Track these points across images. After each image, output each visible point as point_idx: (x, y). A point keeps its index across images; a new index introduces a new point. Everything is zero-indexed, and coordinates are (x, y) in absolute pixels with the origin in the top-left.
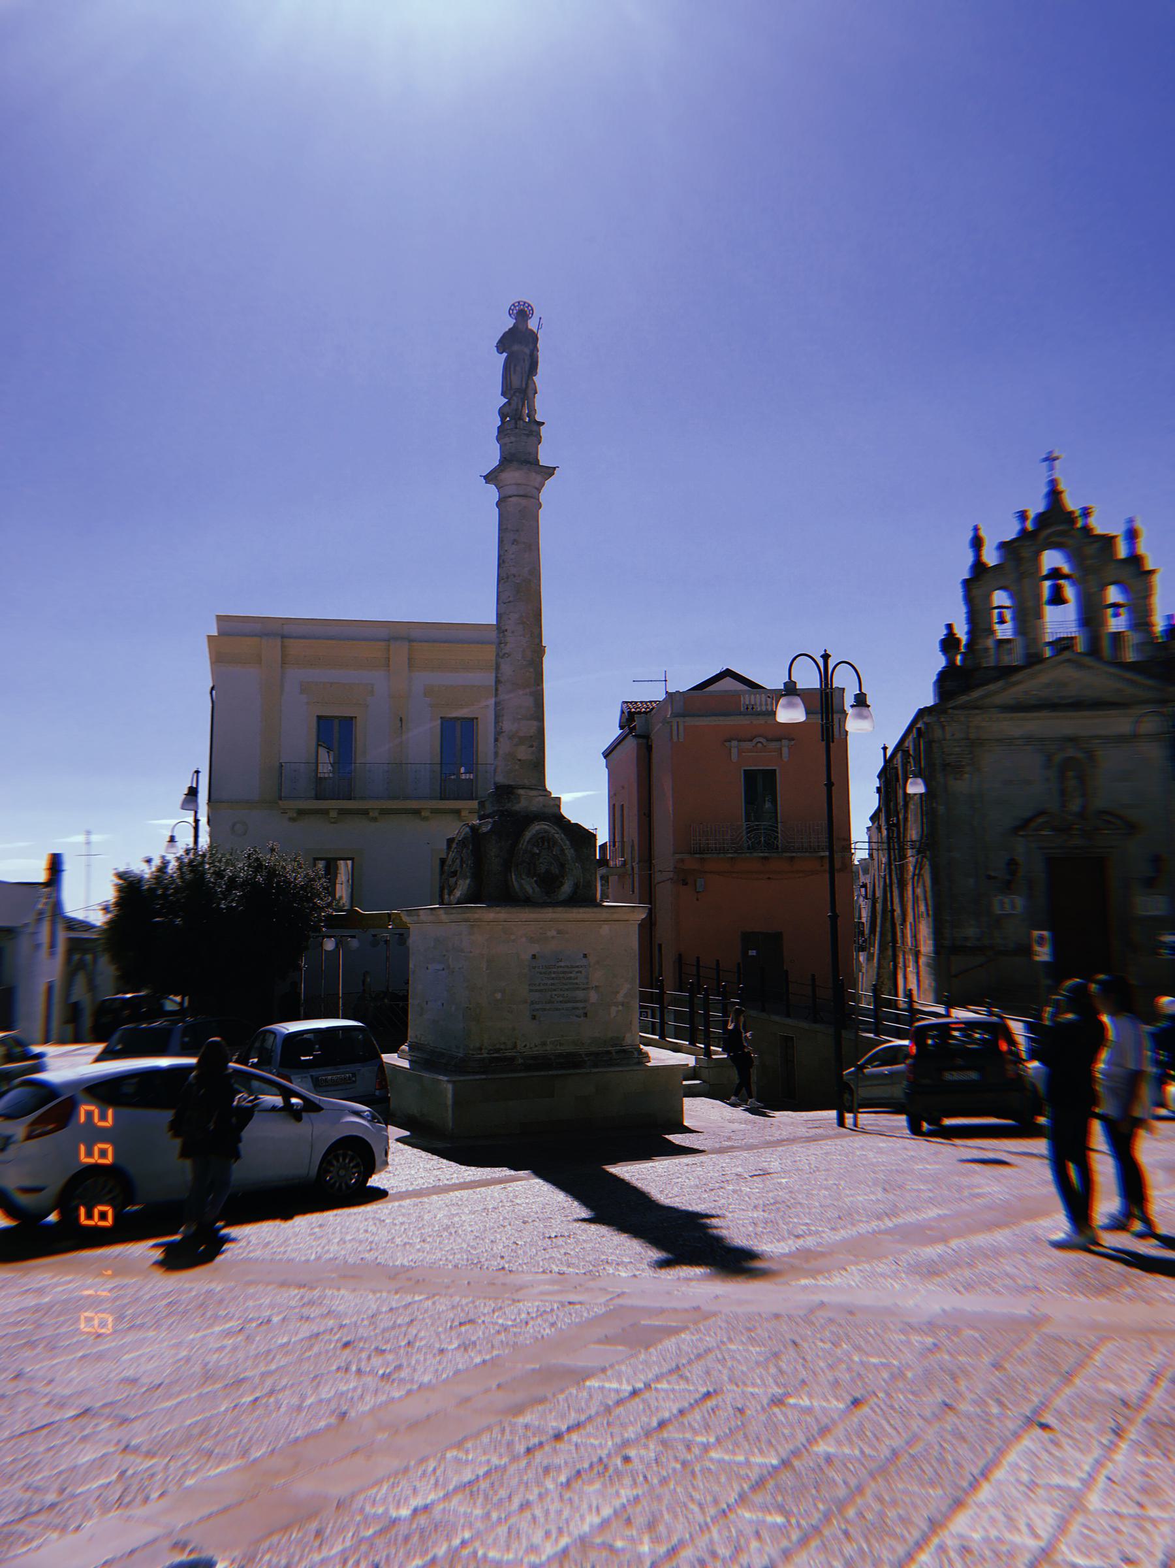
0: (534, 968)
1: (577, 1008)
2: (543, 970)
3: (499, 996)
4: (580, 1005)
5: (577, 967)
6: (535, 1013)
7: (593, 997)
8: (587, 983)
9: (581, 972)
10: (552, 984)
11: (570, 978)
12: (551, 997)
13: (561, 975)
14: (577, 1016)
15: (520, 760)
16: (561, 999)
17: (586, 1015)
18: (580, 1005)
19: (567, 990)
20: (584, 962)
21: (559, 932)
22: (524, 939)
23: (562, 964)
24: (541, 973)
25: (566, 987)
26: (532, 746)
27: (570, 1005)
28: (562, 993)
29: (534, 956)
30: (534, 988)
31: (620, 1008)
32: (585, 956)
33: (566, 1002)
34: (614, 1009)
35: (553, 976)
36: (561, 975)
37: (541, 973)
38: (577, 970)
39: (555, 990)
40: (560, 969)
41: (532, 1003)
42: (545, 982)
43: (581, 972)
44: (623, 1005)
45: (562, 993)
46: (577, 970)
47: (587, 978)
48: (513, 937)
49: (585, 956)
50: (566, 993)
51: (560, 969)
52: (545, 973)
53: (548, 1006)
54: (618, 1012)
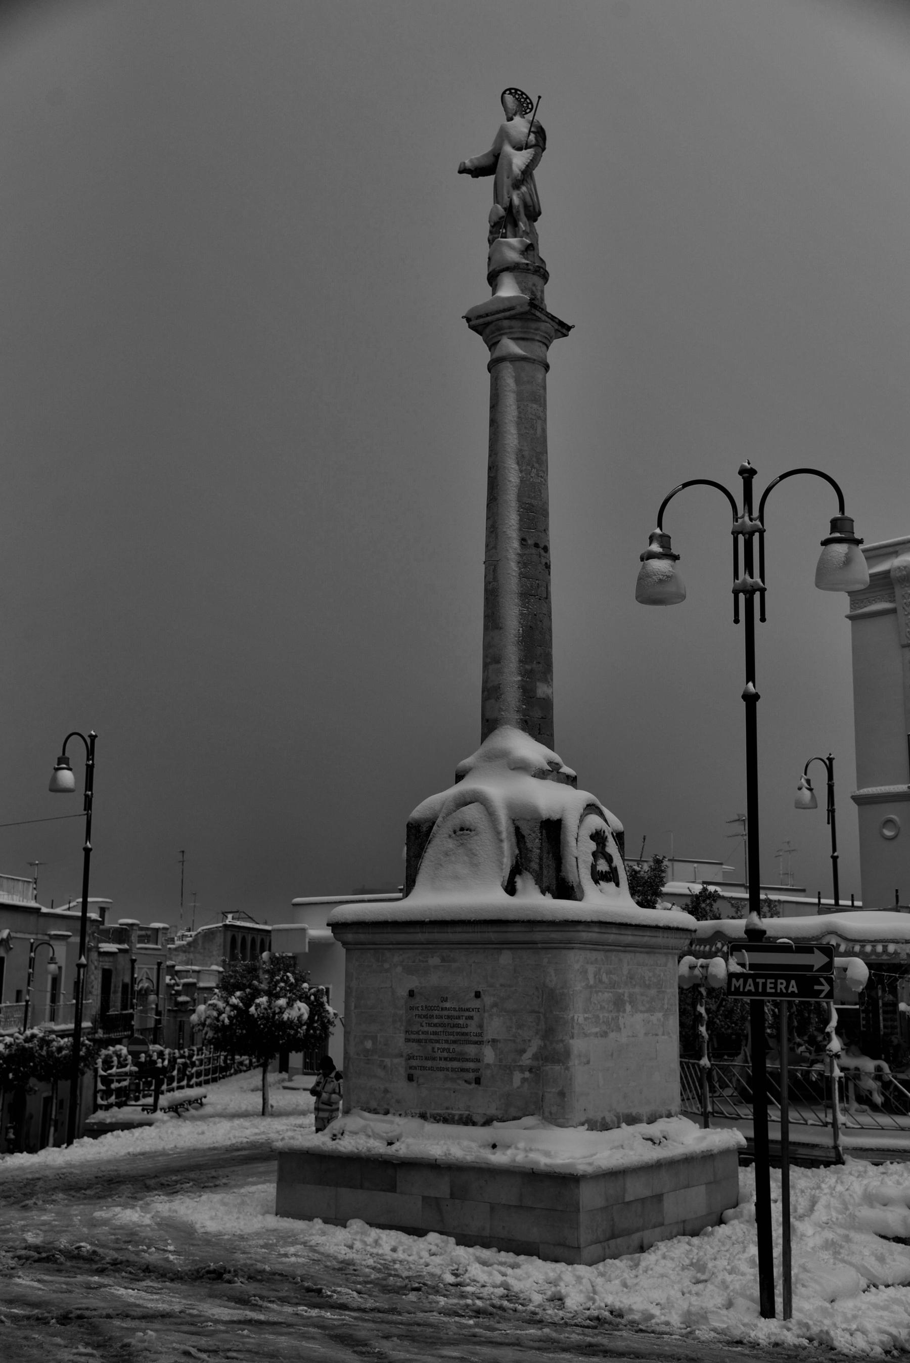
0: (411, 1008)
1: (467, 1070)
2: (424, 1013)
3: (369, 1044)
4: (471, 1065)
5: (468, 1010)
6: (412, 1072)
7: (489, 1055)
8: (480, 1035)
9: (471, 1018)
10: (435, 1033)
11: (458, 1026)
12: (433, 1048)
14: (466, 1081)
16: (445, 1054)
17: (478, 1081)
18: (471, 1065)
19: (455, 1042)
20: (476, 1004)
24: (420, 1016)
25: (451, 1038)
27: (456, 1064)
28: (446, 1046)
29: (411, 994)
30: (413, 1036)
31: (527, 1074)
32: (478, 995)
33: (452, 1059)
34: (517, 1077)
35: (436, 1021)
36: (446, 1021)
37: (420, 1016)
38: (467, 1014)
39: (438, 1041)
40: (446, 1013)
41: (410, 1057)
42: (426, 1029)
43: (471, 1018)
44: (530, 1070)
45: (446, 1046)
46: (467, 1014)
47: (481, 1026)
48: (386, 966)
50: (452, 1047)
51: (446, 1013)
52: (425, 1017)
53: (429, 1064)
54: (524, 1080)
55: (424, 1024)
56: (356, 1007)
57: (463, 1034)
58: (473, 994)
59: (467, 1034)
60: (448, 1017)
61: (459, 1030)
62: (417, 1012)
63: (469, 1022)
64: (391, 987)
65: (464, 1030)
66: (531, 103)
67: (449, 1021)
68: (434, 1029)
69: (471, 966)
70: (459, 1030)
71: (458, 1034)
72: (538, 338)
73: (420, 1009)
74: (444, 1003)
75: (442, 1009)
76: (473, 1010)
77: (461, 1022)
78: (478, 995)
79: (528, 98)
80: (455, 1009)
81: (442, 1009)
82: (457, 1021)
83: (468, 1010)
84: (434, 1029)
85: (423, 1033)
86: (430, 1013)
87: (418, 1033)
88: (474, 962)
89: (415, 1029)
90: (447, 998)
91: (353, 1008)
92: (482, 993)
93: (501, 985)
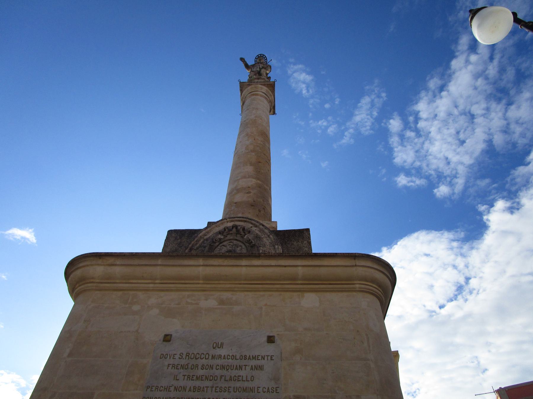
2: (183, 362)
5: (254, 358)
9: (261, 368)
11: (238, 379)
13: (218, 373)
15: (236, 203)
20: (270, 349)
21: (222, 302)
22: (156, 311)
23: (223, 352)
26: (249, 193)
29: (167, 338)
35: (201, 372)
36: (218, 373)
38: (254, 363)
42: (181, 383)
43: (261, 368)
46: (254, 363)
47: (276, 379)
48: (136, 308)
49: (271, 340)
51: (219, 362)
55: (181, 377)
56: (70, 355)
57: (245, 390)
58: (265, 339)
59: (252, 390)
60: (223, 367)
61: (238, 384)
62: (172, 361)
63: (255, 373)
64: (137, 331)
65: (246, 384)
66: (266, 62)
67: (224, 372)
68: (198, 383)
69: (261, 308)
70: (238, 384)
71: (236, 390)
72: (270, 98)
73: (177, 357)
74: (218, 350)
75: (213, 357)
76: (263, 358)
77: (242, 373)
78: (271, 340)
79: (267, 59)
80: (234, 357)
81: (213, 357)
82: (235, 373)
83: (254, 358)
84: (198, 383)
85: (176, 389)
86: (194, 362)
87: (167, 389)
88: (266, 305)
89: (164, 383)
90: (222, 344)
91: (66, 355)
92: (276, 338)
93: (306, 329)
